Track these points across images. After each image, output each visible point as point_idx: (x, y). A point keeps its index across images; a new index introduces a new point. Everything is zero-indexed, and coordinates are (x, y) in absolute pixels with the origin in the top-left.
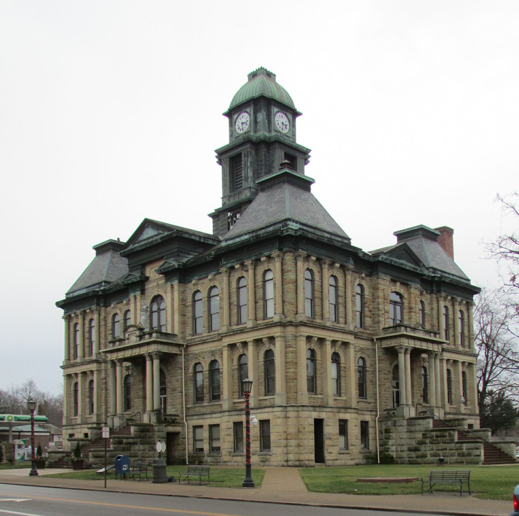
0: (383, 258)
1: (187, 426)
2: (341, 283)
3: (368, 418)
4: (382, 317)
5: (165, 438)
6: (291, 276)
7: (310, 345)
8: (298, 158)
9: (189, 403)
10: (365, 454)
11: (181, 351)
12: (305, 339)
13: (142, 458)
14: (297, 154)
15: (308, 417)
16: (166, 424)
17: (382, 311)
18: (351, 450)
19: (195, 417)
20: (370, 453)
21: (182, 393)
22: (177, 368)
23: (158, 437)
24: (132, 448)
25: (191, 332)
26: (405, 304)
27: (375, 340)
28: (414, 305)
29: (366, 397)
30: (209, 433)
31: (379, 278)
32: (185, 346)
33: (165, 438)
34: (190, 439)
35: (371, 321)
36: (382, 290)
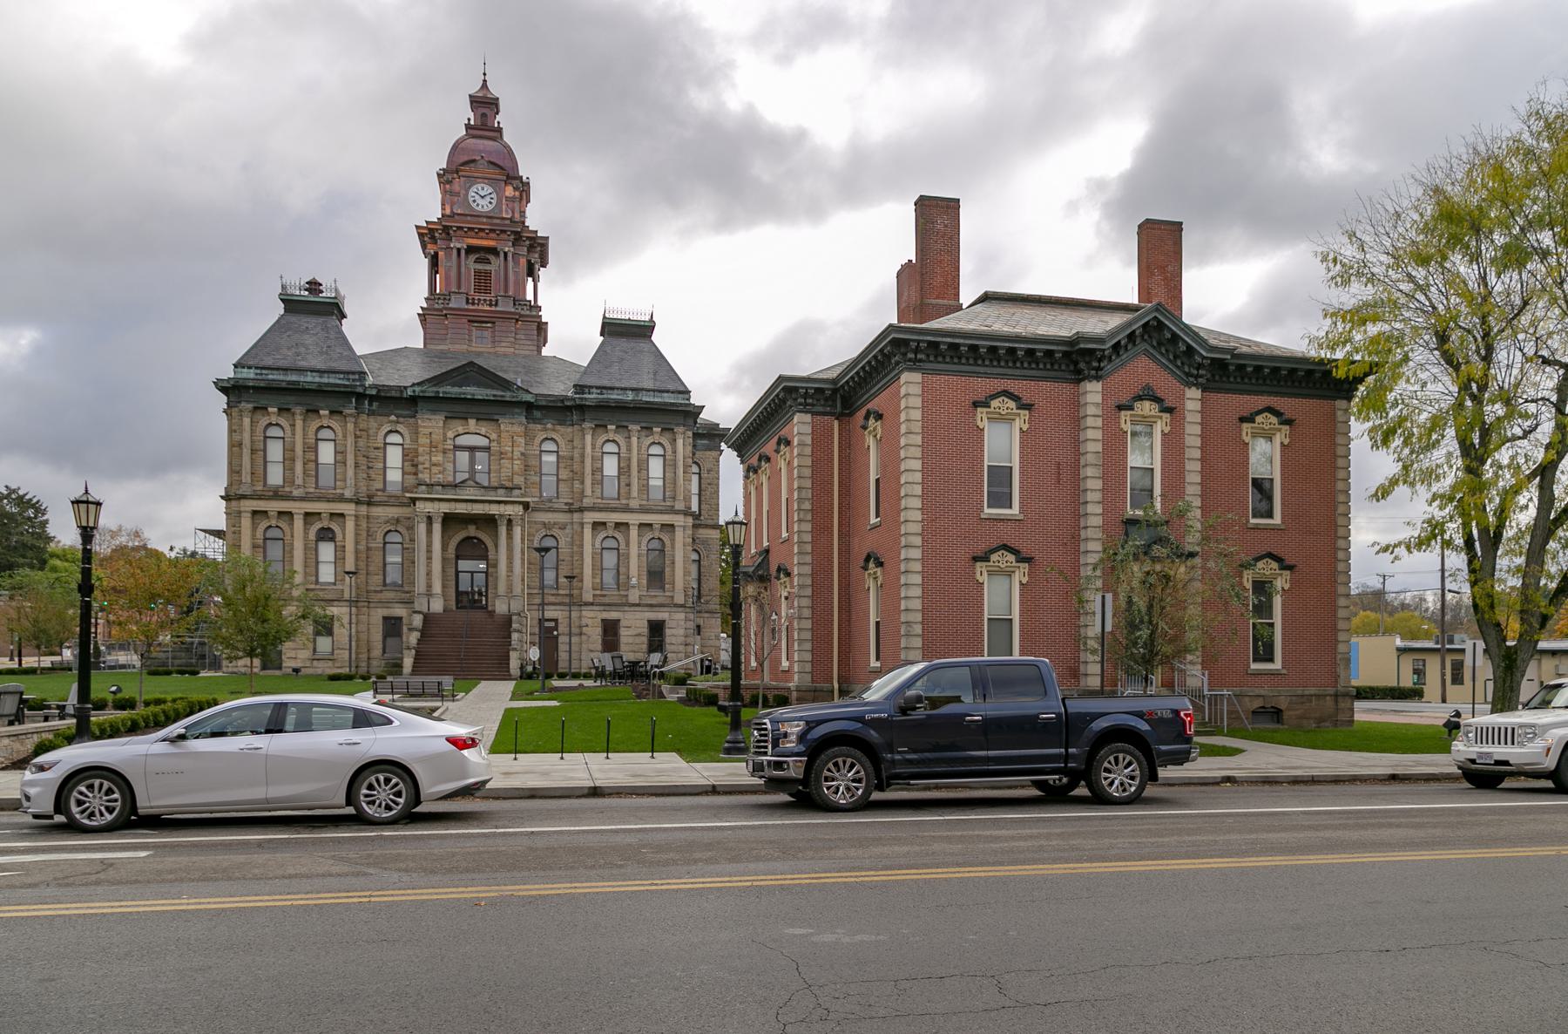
3: (399, 611)
4: (422, 473)
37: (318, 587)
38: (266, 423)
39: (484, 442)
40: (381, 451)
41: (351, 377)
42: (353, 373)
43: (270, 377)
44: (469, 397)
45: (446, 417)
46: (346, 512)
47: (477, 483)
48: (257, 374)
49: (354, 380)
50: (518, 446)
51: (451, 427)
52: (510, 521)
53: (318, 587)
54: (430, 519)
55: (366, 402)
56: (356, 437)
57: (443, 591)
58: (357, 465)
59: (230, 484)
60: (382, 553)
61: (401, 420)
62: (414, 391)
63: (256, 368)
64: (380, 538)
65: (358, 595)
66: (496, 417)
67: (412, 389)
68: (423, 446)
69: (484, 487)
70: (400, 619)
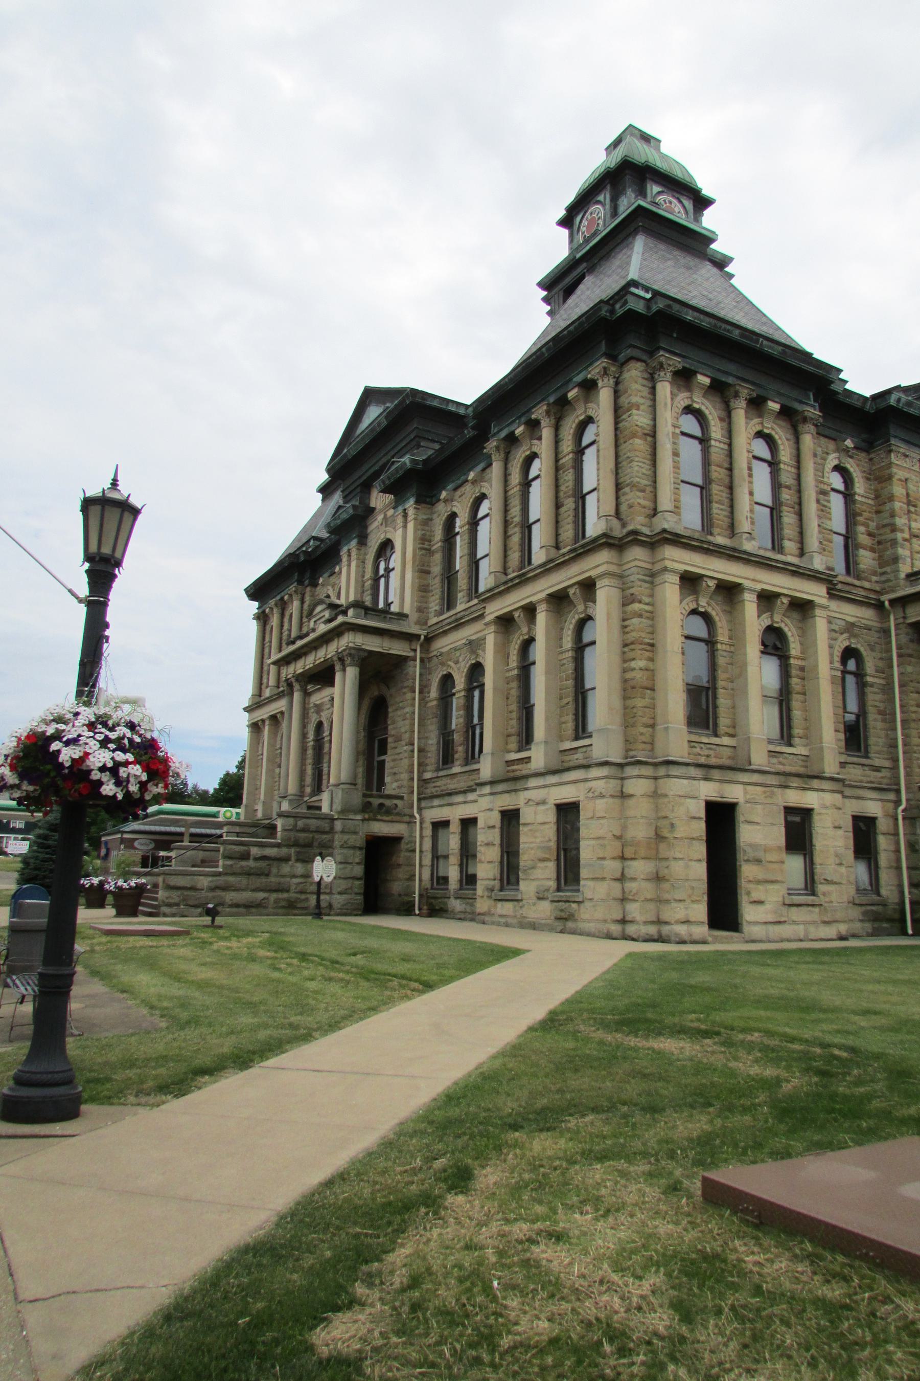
0: (899, 400)
1: (421, 823)
2: (785, 454)
3: (873, 807)
5: (360, 849)
6: (639, 419)
9: (429, 768)
10: (869, 908)
11: (415, 650)
12: (676, 579)
13: (298, 896)
16: (367, 816)
17: (902, 531)
18: (824, 894)
19: (436, 802)
20: (884, 904)
21: (413, 744)
22: (405, 690)
23: (342, 847)
24: (274, 870)
25: (437, 608)
27: (887, 604)
29: (867, 752)
30: (462, 839)
31: (890, 451)
32: (422, 637)
33: (360, 849)
34: (425, 854)
35: (874, 559)
36: (900, 480)
70: (871, 821)
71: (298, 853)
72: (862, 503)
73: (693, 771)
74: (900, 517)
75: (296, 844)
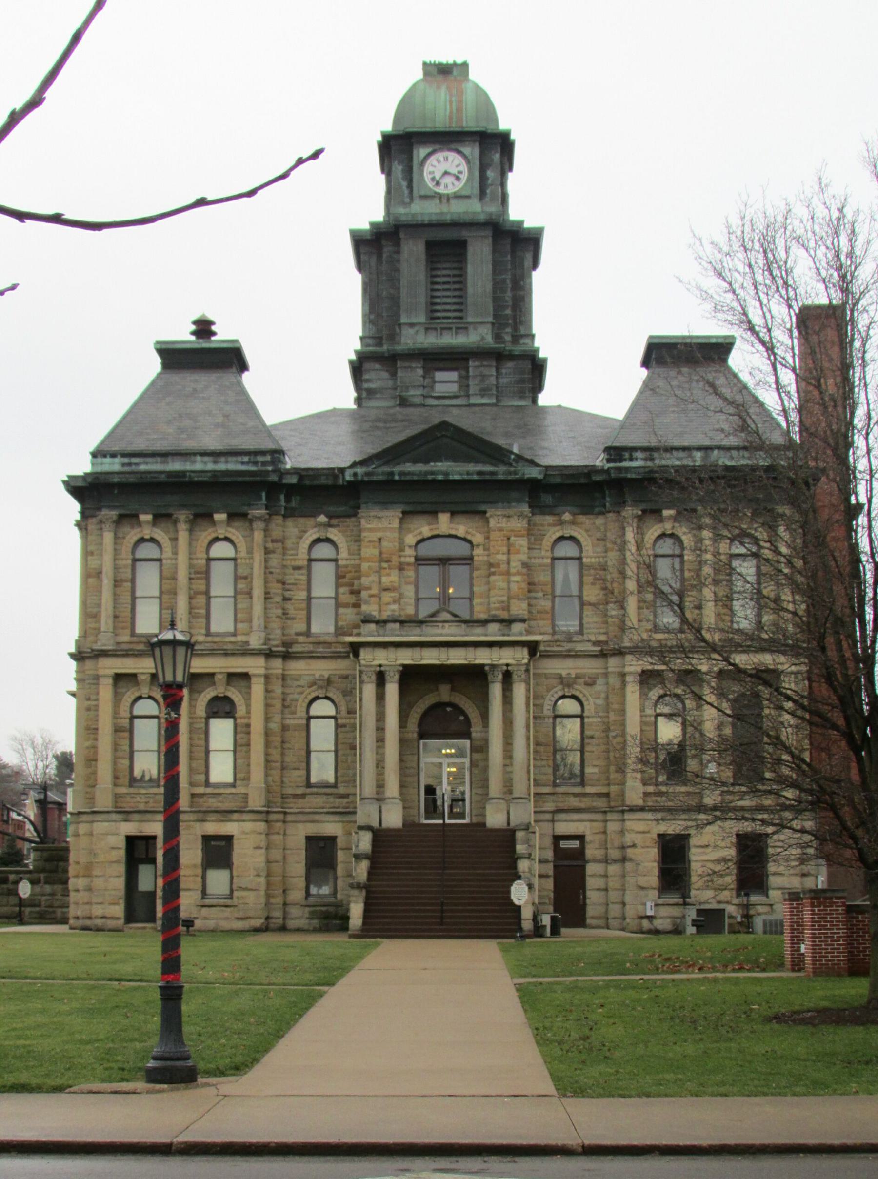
0: (355, 474)
4: (367, 603)
7: (140, 689)
8: (469, 240)
14: (465, 234)
15: (108, 834)
17: (369, 588)
18: (238, 898)
26: (475, 558)
28: (505, 557)
36: (370, 541)
37: (209, 790)
38: (135, 538)
39: (462, 549)
40: (304, 571)
41: (260, 459)
42: (263, 453)
43: (143, 468)
44: (440, 477)
45: (404, 513)
46: (251, 671)
47: (455, 616)
48: (123, 465)
49: (264, 464)
50: (518, 552)
51: (412, 526)
52: (507, 676)
53: (209, 790)
54: (381, 679)
55: (282, 497)
56: (267, 551)
57: (401, 794)
58: (267, 596)
59: (84, 634)
60: (304, 734)
61: (334, 521)
62: (355, 474)
63: (124, 455)
64: (301, 712)
65: (269, 804)
66: (483, 507)
67: (351, 471)
68: (368, 560)
69: (466, 622)
71: (45, 877)
72: (346, 566)
73: (114, 816)
74: (367, 576)
75: (43, 870)
